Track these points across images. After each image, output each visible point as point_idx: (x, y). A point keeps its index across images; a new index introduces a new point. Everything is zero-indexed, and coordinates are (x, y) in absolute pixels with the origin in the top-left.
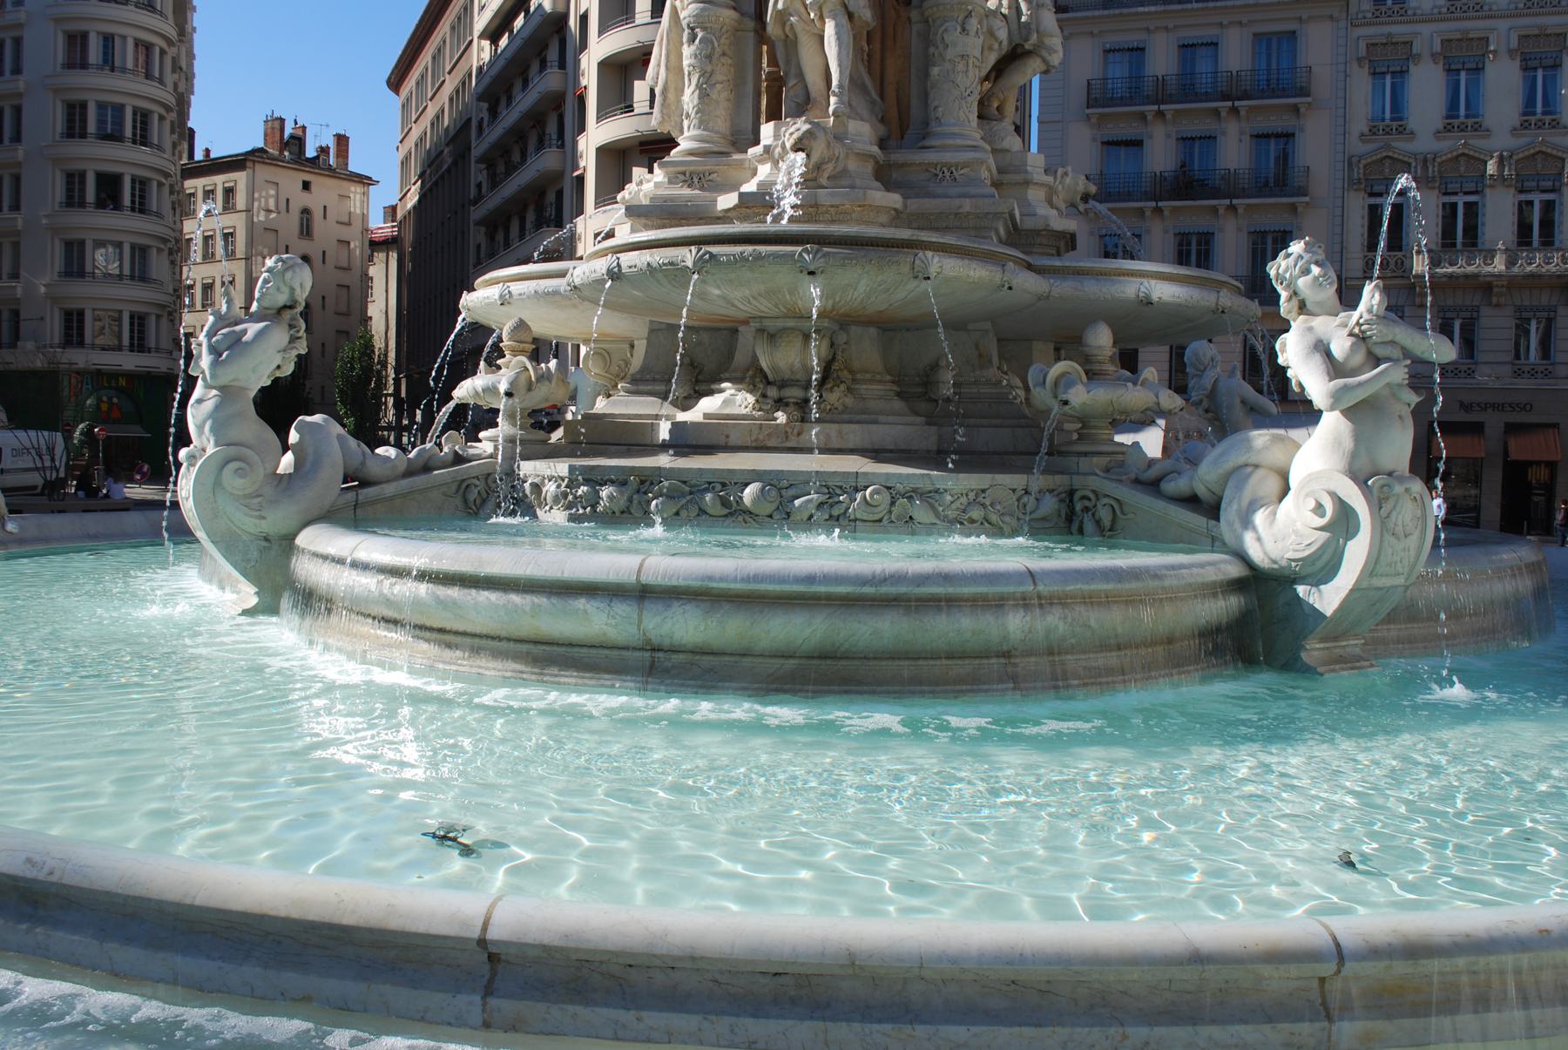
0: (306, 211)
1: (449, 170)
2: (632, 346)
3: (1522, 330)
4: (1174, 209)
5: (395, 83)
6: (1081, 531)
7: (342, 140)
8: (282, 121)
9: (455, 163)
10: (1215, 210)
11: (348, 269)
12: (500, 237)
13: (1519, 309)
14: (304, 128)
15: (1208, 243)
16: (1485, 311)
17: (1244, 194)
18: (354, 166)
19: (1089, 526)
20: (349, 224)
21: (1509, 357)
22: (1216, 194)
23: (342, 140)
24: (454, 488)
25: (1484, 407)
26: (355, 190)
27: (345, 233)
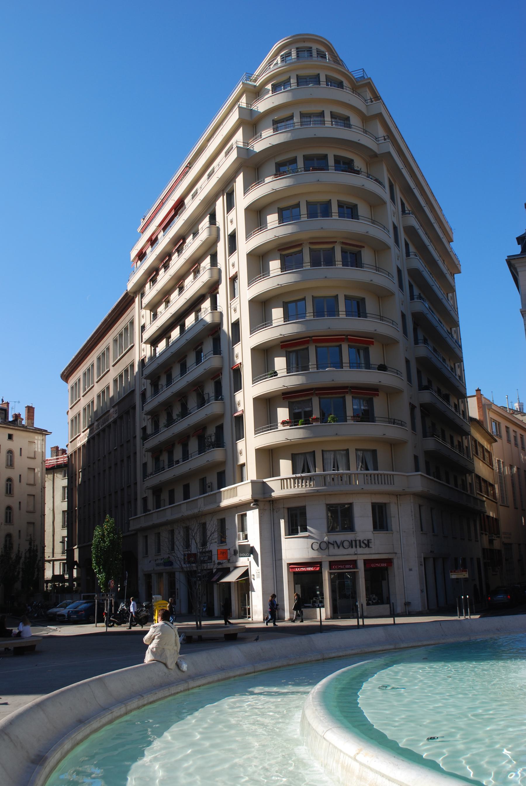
0: (10, 452)
1: (115, 422)
5: (66, 376)
7: (30, 410)
9: (120, 417)
11: (34, 485)
12: (165, 457)
14: (8, 404)
18: (37, 424)
20: (35, 458)
23: (30, 410)
26: (38, 438)
27: (32, 464)
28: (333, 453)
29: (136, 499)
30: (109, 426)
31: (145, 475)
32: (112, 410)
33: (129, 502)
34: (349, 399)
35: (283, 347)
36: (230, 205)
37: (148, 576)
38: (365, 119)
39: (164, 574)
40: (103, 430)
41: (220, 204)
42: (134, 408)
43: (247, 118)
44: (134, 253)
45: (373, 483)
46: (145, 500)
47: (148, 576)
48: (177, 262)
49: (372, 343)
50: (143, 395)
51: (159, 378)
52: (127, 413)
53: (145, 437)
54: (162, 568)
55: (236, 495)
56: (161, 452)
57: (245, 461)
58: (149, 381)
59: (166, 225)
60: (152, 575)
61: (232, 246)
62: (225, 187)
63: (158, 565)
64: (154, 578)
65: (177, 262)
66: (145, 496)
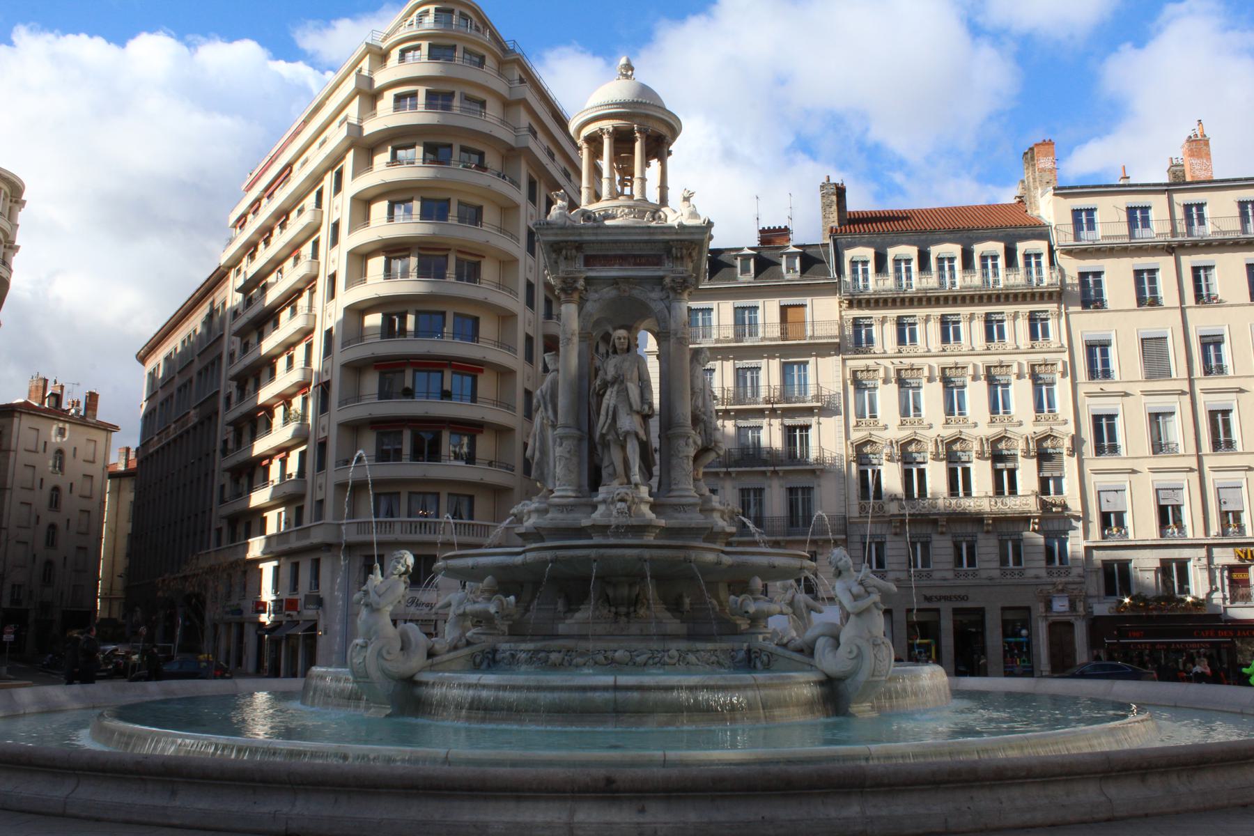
1: (194, 427)
3: (958, 548)
4: (738, 473)
6: (755, 666)
8: (46, 381)
9: (201, 423)
10: (764, 473)
11: (90, 497)
13: (954, 536)
14: (62, 387)
15: (761, 495)
16: (935, 537)
17: (782, 463)
18: (102, 415)
19: (759, 665)
20: (93, 462)
21: (951, 566)
22: (765, 463)
23: (92, 398)
25: (940, 598)
26: (100, 436)
27: (89, 469)
29: (210, 529)
30: (187, 432)
31: (222, 501)
32: (192, 412)
33: (203, 532)
34: (446, 437)
35: (376, 367)
36: (338, 188)
38: (507, 105)
40: (181, 436)
41: (328, 182)
42: (217, 413)
43: (365, 88)
44: (233, 217)
46: (219, 530)
48: (280, 240)
49: (481, 371)
50: (228, 398)
51: (246, 382)
52: (209, 418)
53: (225, 452)
54: (230, 616)
55: (308, 537)
58: (235, 384)
59: (269, 192)
61: (335, 241)
62: (334, 162)
63: (227, 613)
64: (222, 629)
65: (280, 240)
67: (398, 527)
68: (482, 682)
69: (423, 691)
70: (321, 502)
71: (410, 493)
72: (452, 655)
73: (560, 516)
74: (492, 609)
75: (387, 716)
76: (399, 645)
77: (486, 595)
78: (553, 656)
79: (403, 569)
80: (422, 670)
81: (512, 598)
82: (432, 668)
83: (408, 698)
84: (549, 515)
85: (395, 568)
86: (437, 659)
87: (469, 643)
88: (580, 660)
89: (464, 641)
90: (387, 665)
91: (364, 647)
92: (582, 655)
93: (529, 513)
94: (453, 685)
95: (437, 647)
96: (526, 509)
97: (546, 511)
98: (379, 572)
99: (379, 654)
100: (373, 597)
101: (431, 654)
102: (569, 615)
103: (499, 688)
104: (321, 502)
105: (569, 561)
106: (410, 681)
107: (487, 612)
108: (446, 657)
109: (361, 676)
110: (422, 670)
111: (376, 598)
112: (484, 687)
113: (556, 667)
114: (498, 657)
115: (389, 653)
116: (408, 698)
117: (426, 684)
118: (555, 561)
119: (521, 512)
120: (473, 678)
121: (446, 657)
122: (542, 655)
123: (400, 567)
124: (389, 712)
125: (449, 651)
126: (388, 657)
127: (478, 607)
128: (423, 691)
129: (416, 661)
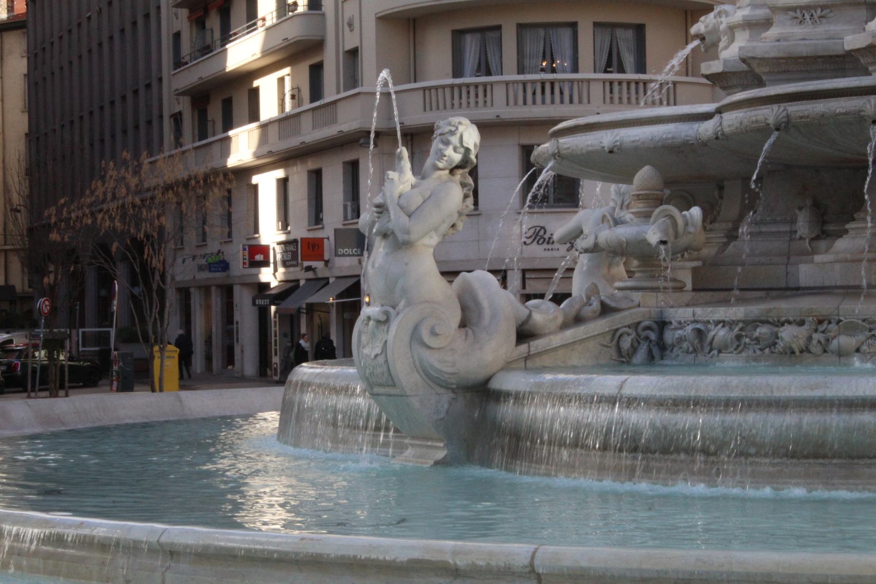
2: (721, 188)
24: (608, 338)
28: (542, 32)
29: (161, 117)
31: (178, 63)
33: (149, 122)
37: (184, 293)
39: (213, 289)
45: (625, 100)
46: (177, 118)
47: (184, 293)
54: (205, 275)
55: (334, 121)
56: (206, 11)
57: (357, 44)
60: (192, 290)
63: (201, 268)
64: (196, 300)
66: (177, 110)
67: (499, 93)
68: (627, 391)
69: (507, 411)
70: (354, 53)
71: (521, 27)
72: (570, 334)
73: (798, 31)
74: (653, 236)
75: (437, 463)
76: (456, 317)
77: (639, 207)
78: (787, 333)
79: (457, 157)
80: (508, 366)
81: (696, 212)
82: (527, 363)
83: (479, 426)
84: (773, 32)
85: (441, 155)
86: (537, 345)
87: (606, 310)
88: (845, 341)
89: (596, 305)
90: (432, 359)
91: (384, 322)
92: (851, 329)
93: (732, 29)
94: (577, 394)
95: (538, 317)
96: (724, 22)
97: (767, 23)
98: (406, 164)
99: (415, 336)
100: (396, 219)
101: (524, 334)
102: (822, 244)
103: (660, 403)
104: (354, 53)
105: (813, 127)
106: (482, 392)
107: (644, 242)
108: (557, 340)
109: (381, 383)
110: (508, 366)
111: (404, 219)
112: (631, 402)
113: (792, 356)
114: (670, 336)
115: (434, 333)
116: (479, 426)
117: (519, 398)
118: (784, 126)
119: (715, 30)
120: (609, 383)
121: (557, 340)
122: (763, 330)
123: (449, 151)
124: (441, 455)
125: (564, 326)
126: (427, 338)
127: (623, 233)
128: (507, 411)
129: (493, 349)
